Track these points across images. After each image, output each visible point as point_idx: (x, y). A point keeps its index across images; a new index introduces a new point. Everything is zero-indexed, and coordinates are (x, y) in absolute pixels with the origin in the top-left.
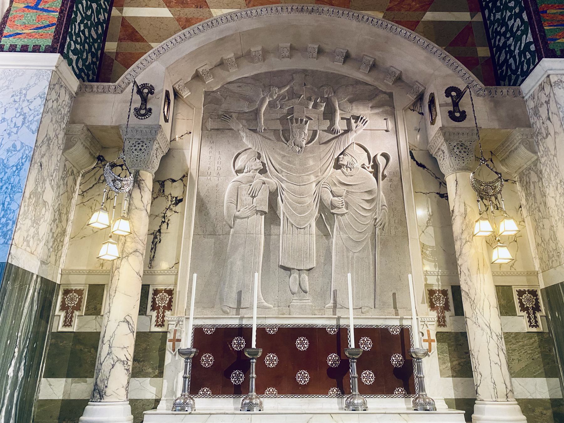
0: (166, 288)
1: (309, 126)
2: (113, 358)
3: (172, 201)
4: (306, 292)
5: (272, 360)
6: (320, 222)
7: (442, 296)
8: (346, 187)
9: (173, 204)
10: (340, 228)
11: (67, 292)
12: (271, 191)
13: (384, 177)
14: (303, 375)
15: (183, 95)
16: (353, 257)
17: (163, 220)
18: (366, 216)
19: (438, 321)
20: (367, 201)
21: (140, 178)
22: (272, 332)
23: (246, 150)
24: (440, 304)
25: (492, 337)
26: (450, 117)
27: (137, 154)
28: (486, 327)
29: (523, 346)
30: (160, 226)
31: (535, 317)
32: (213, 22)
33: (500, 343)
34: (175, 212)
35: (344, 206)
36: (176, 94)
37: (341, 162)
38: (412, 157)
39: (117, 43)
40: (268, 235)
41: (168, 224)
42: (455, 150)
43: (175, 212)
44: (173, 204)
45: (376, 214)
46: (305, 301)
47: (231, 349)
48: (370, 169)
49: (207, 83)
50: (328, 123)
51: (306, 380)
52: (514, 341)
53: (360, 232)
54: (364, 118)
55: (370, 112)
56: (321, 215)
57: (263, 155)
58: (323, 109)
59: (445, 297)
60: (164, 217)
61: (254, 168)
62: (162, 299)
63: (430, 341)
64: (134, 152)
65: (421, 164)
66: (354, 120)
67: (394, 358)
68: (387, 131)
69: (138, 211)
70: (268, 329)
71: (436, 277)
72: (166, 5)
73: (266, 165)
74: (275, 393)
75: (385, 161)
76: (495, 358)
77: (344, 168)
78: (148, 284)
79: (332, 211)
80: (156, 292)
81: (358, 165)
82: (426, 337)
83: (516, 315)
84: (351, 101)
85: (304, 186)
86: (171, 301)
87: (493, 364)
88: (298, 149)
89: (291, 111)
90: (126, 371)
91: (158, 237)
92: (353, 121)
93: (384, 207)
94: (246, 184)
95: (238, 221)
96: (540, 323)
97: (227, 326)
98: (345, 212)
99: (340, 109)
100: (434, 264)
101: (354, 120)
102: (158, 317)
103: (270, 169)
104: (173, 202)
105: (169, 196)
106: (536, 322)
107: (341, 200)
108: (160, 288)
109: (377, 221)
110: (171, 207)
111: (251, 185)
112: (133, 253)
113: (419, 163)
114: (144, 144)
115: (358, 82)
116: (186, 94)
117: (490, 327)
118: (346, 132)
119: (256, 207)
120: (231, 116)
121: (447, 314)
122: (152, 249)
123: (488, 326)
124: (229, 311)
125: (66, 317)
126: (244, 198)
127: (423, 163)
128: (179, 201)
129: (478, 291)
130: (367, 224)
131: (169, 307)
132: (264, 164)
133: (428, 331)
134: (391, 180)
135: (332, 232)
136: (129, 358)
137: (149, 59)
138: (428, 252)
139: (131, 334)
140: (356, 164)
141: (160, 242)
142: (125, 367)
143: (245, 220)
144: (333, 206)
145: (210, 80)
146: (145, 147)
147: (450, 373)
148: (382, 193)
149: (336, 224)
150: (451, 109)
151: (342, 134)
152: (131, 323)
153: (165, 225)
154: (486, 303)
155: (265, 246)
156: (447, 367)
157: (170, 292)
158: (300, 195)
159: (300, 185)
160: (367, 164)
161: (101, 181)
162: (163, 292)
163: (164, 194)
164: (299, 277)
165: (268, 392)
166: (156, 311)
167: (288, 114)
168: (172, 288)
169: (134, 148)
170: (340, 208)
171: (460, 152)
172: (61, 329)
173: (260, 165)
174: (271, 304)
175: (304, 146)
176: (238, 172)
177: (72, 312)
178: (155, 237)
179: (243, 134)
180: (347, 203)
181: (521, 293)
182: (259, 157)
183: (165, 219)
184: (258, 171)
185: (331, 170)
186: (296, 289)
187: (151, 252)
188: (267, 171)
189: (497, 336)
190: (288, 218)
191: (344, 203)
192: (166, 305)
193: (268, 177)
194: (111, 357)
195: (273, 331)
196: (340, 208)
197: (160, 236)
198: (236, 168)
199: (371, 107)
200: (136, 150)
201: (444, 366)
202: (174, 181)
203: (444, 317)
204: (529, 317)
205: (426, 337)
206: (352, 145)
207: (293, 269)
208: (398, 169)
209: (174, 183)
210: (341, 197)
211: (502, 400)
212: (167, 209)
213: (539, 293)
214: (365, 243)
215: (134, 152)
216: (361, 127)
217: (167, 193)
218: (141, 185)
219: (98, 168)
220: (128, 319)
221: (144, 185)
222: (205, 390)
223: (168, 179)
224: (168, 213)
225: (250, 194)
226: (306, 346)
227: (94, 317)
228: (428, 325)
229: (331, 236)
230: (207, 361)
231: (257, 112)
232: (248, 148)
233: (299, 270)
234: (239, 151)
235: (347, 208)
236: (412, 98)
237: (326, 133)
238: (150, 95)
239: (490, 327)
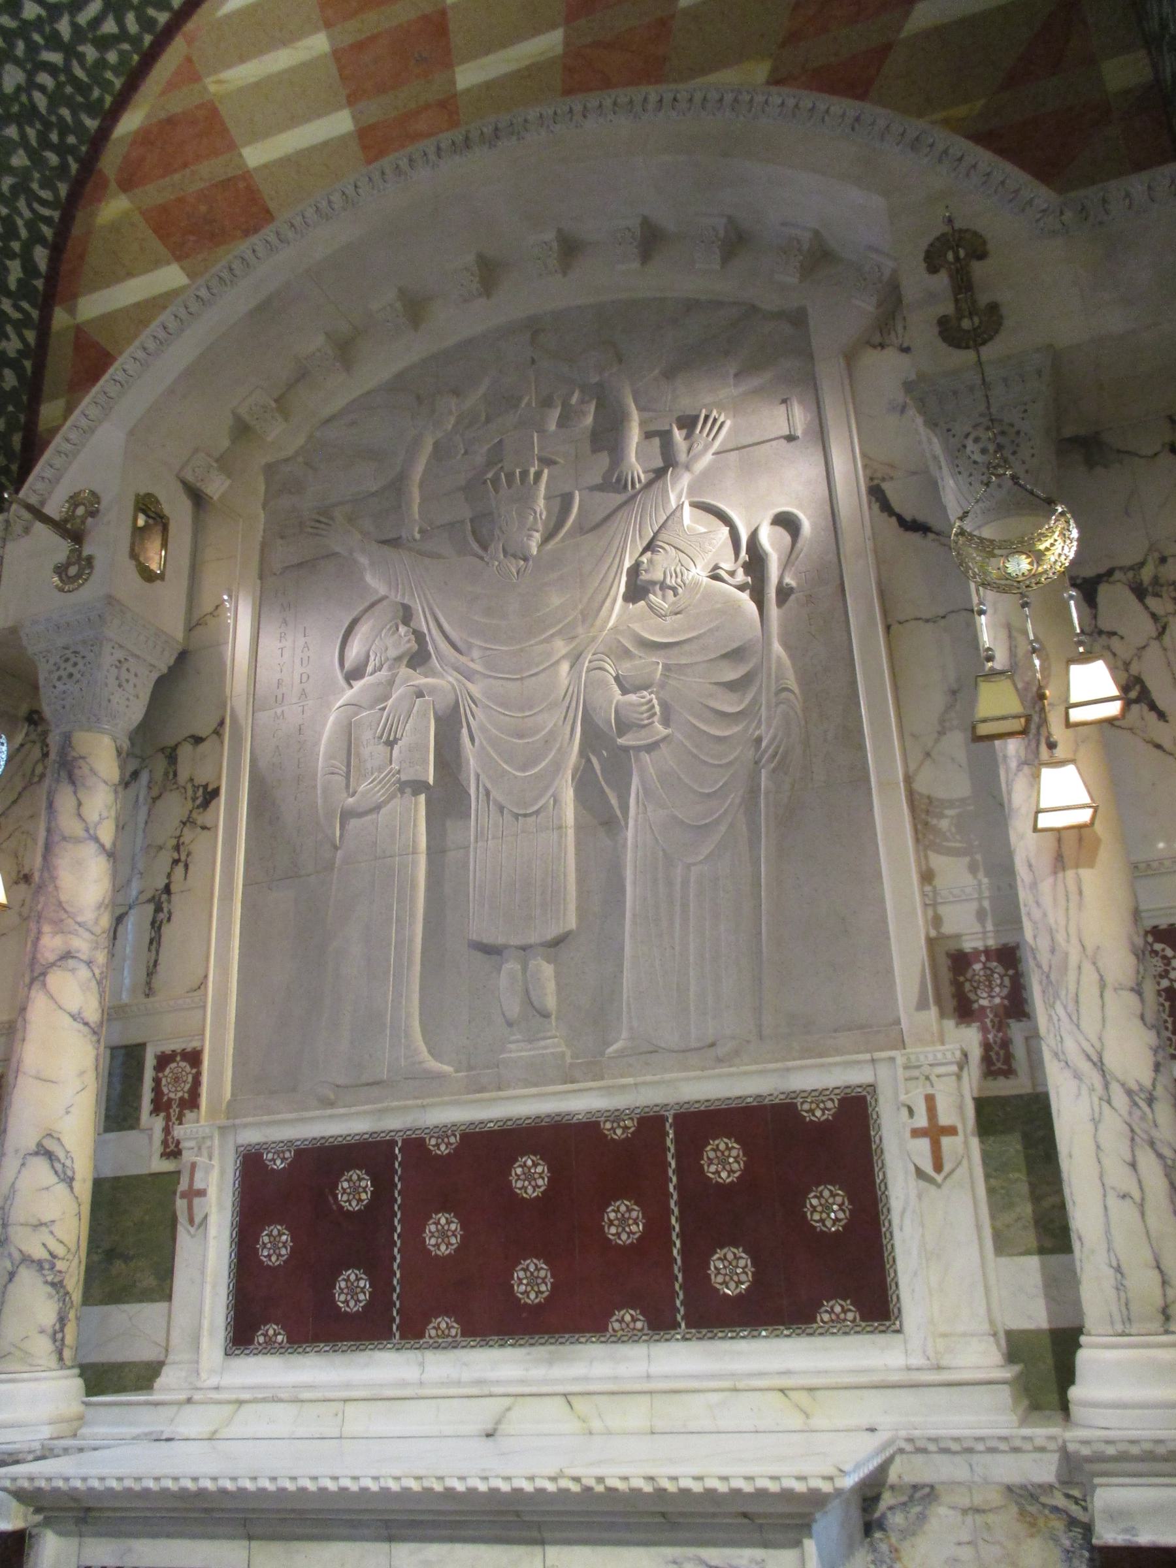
0: (183, 1046)
1: (548, 487)
2: (10, 1255)
3: (194, 799)
4: (546, 1015)
5: (444, 1234)
6: (585, 783)
7: (1000, 970)
8: (662, 652)
9: (198, 807)
10: (647, 791)
12: (440, 713)
13: (784, 593)
14: (532, 1273)
15: (210, 494)
16: (685, 883)
17: (176, 856)
18: (725, 738)
19: (987, 1060)
20: (731, 686)
21: (74, 754)
22: (443, 1147)
23: (372, 605)
24: (988, 1000)
25: (1109, 1102)
26: (945, 339)
27: (64, 688)
28: (1085, 1067)
30: (169, 876)
32: (234, 266)
33: (1143, 1118)
34: (204, 828)
35: (656, 719)
36: (197, 498)
37: (644, 576)
38: (886, 507)
39: (64, 400)
40: (436, 852)
41: (186, 866)
42: (969, 449)
44: (198, 807)
45: (758, 726)
46: (542, 1043)
47: (334, 1207)
48: (741, 577)
49: (269, 439)
50: (604, 459)
51: (543, 1288)
53: (709, 795)
54: (715, 413)
55: (735, 392)
56: (589, 761)
57: (418, 607)
58: (589, 420)
59: (1011, 972)
60: (177, 848)
61: (393, 653)
62: (177, 1080)
63: (935, 1133)
64: (58, 684)
65: (914, 521)
66: (684, 432)
67: (815, 1202)
68: (790, 438)
69: (69, 846)
70: (433, 1142)
71: (974, 906)
72: (173, 254)
73: (428, 638)
74: (453, 1332)
75: (787, 538)
77: (655, 595)
78: (140, 1040)
79: (620, 741)
81: (698, 573)
82: (922, 1121)
84: (669, 374)
85: (533, 678)
86: (197, 1083)
88: (513, 566)
89: (496, 455)
90: (49, 1289)
91: (165, 905)
92: (678, 435)
93: (784, 695)
94: (371, 707)
95: (354, 823)
97: (323, 1141)
98: (658, 737)
99: (641, 409)
100: (966, 860)
101: (684, 432)
103: (436, 648)
104: (198, 802)
105: (189, 786)
107: (648, 697)
108: (168, 1048)
109: (764, 744)
110: (194, 815)
111: (384, 709)
112: (59, 963)
113: (908, 518)
114: (79, 660)
115: (691, 306)
116: (216, 487)
117: (1099, 1065)
118: (659, 474)
119: (399, 772)
120: (332, 519)
122: (151, 942)
123: (1095, 1058)
124: (332, 1097)
126: (366, 752)
127: (921, 517)
128: (211, 795)
129: (1060, 938)
130: (730, 763)
131: (191, 1101)
132: (419, 636)
133: (930, 1100)
134: (810, 599)
135: (625, 808)
136: (60, 1251)
137: (84, 422)
138: (944, 824)
139: (62, 1188)
140: (694, 571)
141: (169, 919)
142: (44, 1276)
143: (369, 818)
144: (623, 726)
145: (275, 430)
146: (80, 666)
147: (1030, 1238)
148: (777, 647)
149: (635, 782)
150: (948, 308)
151: (650, 484)
152: (61, 1155)
153: (179, 870)
154: (1090, 977)
155: (429, 889)
156: (1019, 1219)
158: (522, 709)
159: (522, 679)
160: (727, 565)
161: (36, 779)
162: (178, 1058)
163: (175, 783)
164: (525, 969)
165: (433, 1333)
166: (162, 1115)
167: (490, 464)
168: (190, 1046)
169: (56, 675)
170: (644, 726)
171: (984, 451)
173: (409, 641)
174: (448, 1064)
175: (534, 551)
176: (353, 675)
178: (158, 909)
179: (363, 560)
180: (665, 706)
182: (406, 615)
183: (179, 853)
184: (405, 662)
185: (616, 610)
186: (513, 1007)
187: (149, 950)
188: (430, 655)
189: (1129, 1093)
190: (489, 786)
191: (657, 708)
192: (186, 1096)
193: (433, 673)
194: (6, 1253)
195: (448, 1144)
196: (644, 726)
197: (169, 902)
198: (348, 665)
199: (736, 375)
200: (60, 679)
201: (1008, 1217)
202: (198, 740)
203: (1006, 1044)
205: (922, 1121)
206: (678, 514)
207: (506, 947)
208: (832, 556)
210: (646, 688)
211: (1144, 1331)
212: (184, 824)
214: (723, 828)
215: (58, 684)
216: (706, 448)
217: (183, 775)
218: (76, 771)
219: (27, 746)
220: (50, 1144)
221: (86, 770)
222: (271, 1332)
223: (185, 740)
225: (381, 737)
226: (540, 1182)
228: (933, 1078)
229: (623, 823)
230: (275, 1247)
231: (398, 486)
232: (379, 596)
233: (524, 948)
234: (355, 614)
235: (666, 722)
236: (867, 305)
237: (598, 496)
238: (90, 520)
239: (1099, 1065)
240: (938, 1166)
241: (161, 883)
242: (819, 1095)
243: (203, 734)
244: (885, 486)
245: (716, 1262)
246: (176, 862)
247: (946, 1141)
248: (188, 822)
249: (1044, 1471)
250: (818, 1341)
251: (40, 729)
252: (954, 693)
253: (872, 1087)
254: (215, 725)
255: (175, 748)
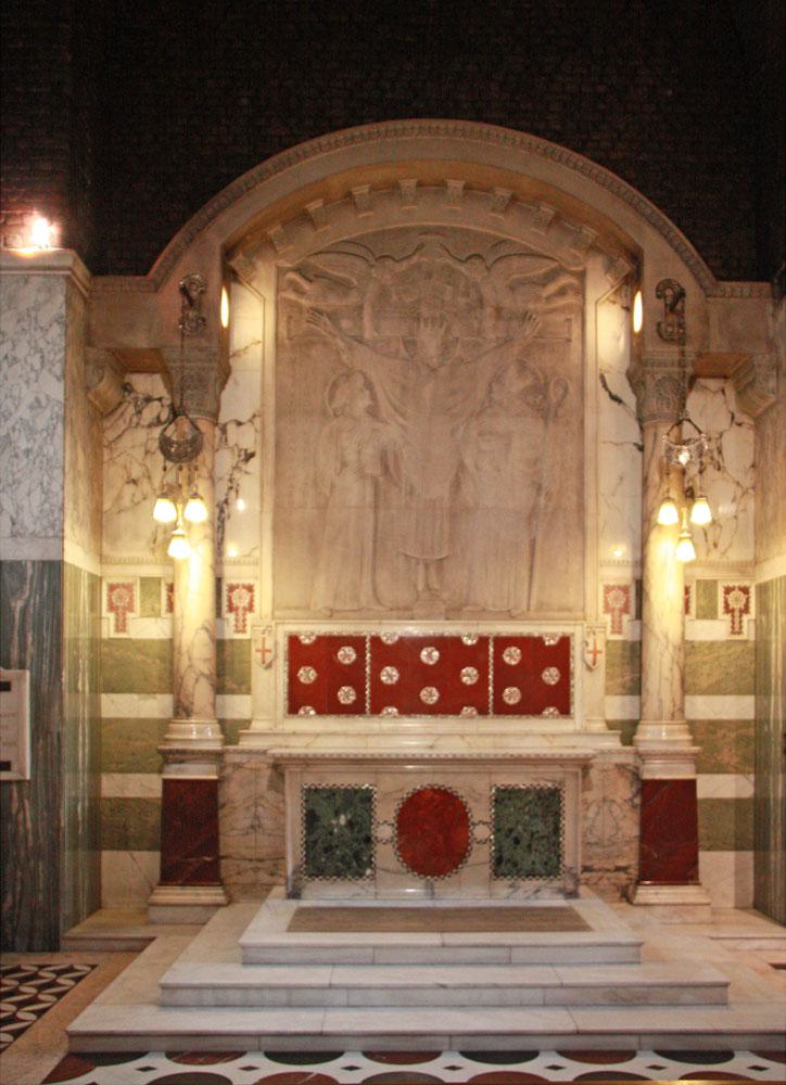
3: (239, 456)
11: (112, 588)
29: (718, 657)
31: (741, 622)
34: (247, 473)
41: (237, 492)
43: (247, 473)
52: (707, 652)
54: (534, 317)
60: (231, 481)
76: (666, 673)
80: (232, 588)
83: (716, 618)
87: (663, 681)
91: (226, 511)
96: (745, 630)
102: (237, 620)
106: (741, 628)
110: (240, 465)
121: (626, 618)
122: (219, 528)
125: (117, 620)
127: (619, 395)
131: (250, 608)
153: (233, 493)
157: (250, 589)
168: (251, 582)
172: (113, 635)
177: (124, 614)
178: (222, 511)
181: (728, 591)
201: (611, 683)
203: (620, 622)
204: (733, 622)
209: (242, 427)
213: (753, 591)
217: (231, 442)
224: (237, 475)
227: (153, 620)
239: (666, 637)
240: (594, 664)
241: (224, 498)
242: (552, 636)
243: (243, 421)
244: (606, 375)
245: (507, 691)
246: (231, 488)
247: (599, 656)
248: (236, 468)
249: (630, 760)
250: (543, 721)
251: (132, 395)
252: (621, 478)
253: (573, 634)
254: (248, 417)
255: (225, 425)
